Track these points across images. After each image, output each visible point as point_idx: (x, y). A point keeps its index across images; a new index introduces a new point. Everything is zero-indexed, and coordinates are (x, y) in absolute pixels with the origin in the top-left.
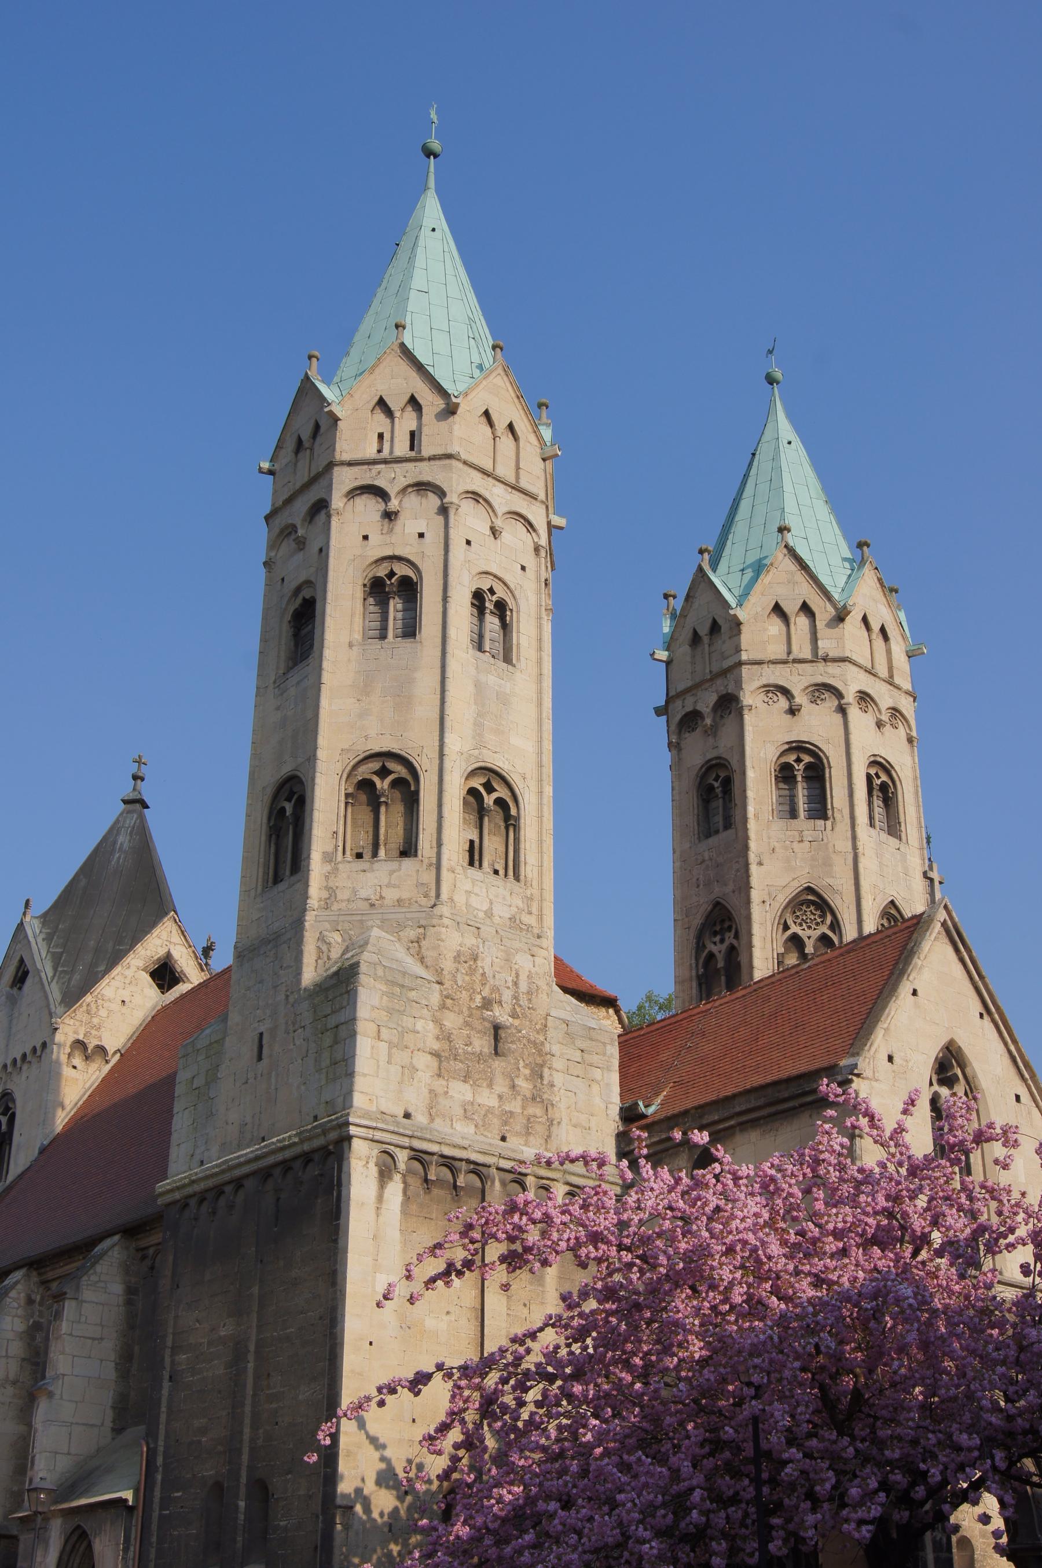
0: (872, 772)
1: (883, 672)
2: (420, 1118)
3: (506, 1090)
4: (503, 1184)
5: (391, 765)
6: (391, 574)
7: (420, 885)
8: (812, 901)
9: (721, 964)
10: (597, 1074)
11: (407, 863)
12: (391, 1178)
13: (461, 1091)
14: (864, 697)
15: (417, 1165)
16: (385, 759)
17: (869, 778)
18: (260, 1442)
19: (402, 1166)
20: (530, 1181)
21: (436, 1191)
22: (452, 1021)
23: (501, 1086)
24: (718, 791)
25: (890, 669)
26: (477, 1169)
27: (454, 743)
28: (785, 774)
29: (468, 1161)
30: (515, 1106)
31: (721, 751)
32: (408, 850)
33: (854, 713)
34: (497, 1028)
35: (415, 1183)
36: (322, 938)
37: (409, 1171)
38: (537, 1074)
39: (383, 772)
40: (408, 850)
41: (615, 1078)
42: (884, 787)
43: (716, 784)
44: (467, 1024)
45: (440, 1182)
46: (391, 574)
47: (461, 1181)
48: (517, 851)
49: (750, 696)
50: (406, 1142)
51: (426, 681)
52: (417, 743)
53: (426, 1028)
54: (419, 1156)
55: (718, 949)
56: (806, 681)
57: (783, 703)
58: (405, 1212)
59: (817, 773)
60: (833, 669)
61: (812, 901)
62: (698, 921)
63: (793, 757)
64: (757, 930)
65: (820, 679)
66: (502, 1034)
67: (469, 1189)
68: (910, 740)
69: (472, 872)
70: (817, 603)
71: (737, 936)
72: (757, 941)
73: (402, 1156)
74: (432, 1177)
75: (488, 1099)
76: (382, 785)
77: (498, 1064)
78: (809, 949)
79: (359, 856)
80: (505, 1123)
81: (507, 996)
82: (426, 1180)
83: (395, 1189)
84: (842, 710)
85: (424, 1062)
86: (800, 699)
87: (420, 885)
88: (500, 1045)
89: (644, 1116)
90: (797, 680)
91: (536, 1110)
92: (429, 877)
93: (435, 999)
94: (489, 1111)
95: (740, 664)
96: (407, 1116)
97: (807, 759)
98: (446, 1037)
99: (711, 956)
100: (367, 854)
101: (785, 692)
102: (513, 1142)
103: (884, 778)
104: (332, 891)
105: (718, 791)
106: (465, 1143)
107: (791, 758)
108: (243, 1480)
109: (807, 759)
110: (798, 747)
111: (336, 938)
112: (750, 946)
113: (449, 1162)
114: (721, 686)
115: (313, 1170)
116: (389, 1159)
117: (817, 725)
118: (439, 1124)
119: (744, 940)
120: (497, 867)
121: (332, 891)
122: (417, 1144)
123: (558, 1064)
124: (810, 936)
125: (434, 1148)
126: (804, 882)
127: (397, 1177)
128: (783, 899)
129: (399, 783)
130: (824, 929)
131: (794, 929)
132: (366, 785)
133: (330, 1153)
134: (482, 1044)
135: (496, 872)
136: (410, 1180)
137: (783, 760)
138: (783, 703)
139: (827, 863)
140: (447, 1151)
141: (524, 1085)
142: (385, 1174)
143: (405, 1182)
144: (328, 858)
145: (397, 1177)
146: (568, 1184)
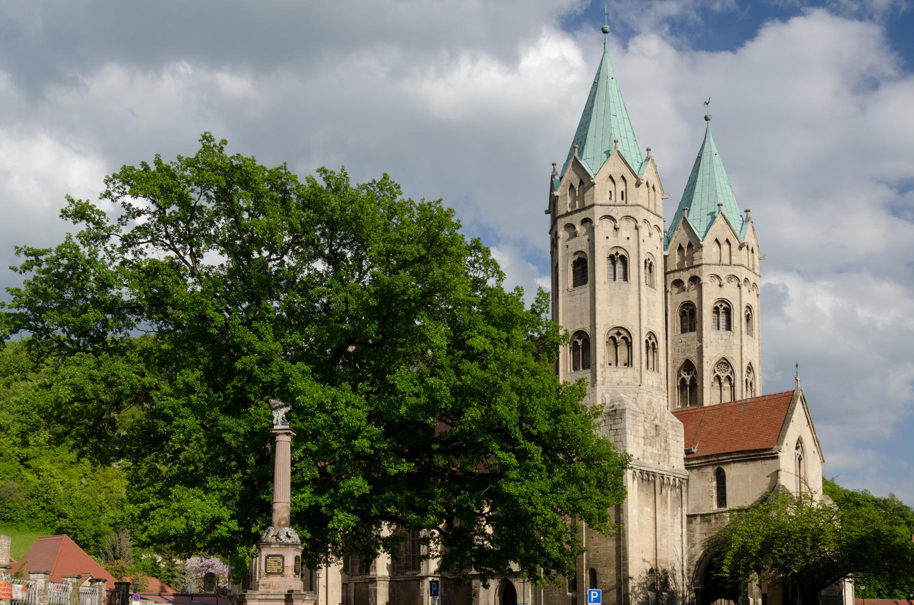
1: (751, 268)
2: (641, 459)
5: (621, 331)
6: (617, 254)
7: (634, 378)
8: (725, 363)
9: (688, 383)
11: (630, 370)
14: (746, 280)
16: (619, 329)
22: (647, 425)
23: (658, 447)
25: (753, 265)
26: (654, 474)
27: (644, 324)
28: (716, 310)
30: (661, 453)
32: (629, 363)
33: (743, 287)
36: (603, 396)
38: (666, 441)
39: (619, 334)
40: (629, 363)
46: (617, 254)
48: (658, 361)
49: (705, 279)
51: (633, 300)
52: (631, 325)
53: (641, 429)
54: (641, 472)
55: (688, 378)
56: (726, 274)
57: (717, 282)
59: (728, 311)
60: (737, 269)
61: (725, 363)
62: (679, 365)
64: (705, 373)
65: (732, 273)
68: (758, 295)
70: (732, 240)
71: (695, 373)
72: (705, 377)
73: (638, 472)
76: (618, 339)
77: (657, 439)
78: (722, 381)
79: (610, 364)
81: (658, 415)
83: (636, 481)
84: (739, 286)
85: (641, 441)
86: (724, 281)
87: (634, 378)
90: (724, 273)
91: (666, 453)
92: (637, 375)
93: (643, 419)
95: (702, 264)
97: (725, 305)
98: (645, 431)
99: (683, 379)
100: (614, 363)
101: (718, 277)
104: (604, 378)
107: (718, 305)
109: (725, 305)
110: (722, 301)
111: (607, 396)
112: (702, 379)
113: (648, 473)
114: (693, 272)
117: (730, 292)
118: (645, 461)
119: (699, 376)
121: (604, 378)
123: (670, 437)
124: (723, 375)
126: (722, 355)
128: (714, 361)
129: (624, 338)
130: (728, 373)
131: (718, 373)
132: (613, 338)
134: (653, 433)
138: (717, 282)
139: (731, 348)
141: (663, 445)
142: (634, 479)
144: (602, 366)
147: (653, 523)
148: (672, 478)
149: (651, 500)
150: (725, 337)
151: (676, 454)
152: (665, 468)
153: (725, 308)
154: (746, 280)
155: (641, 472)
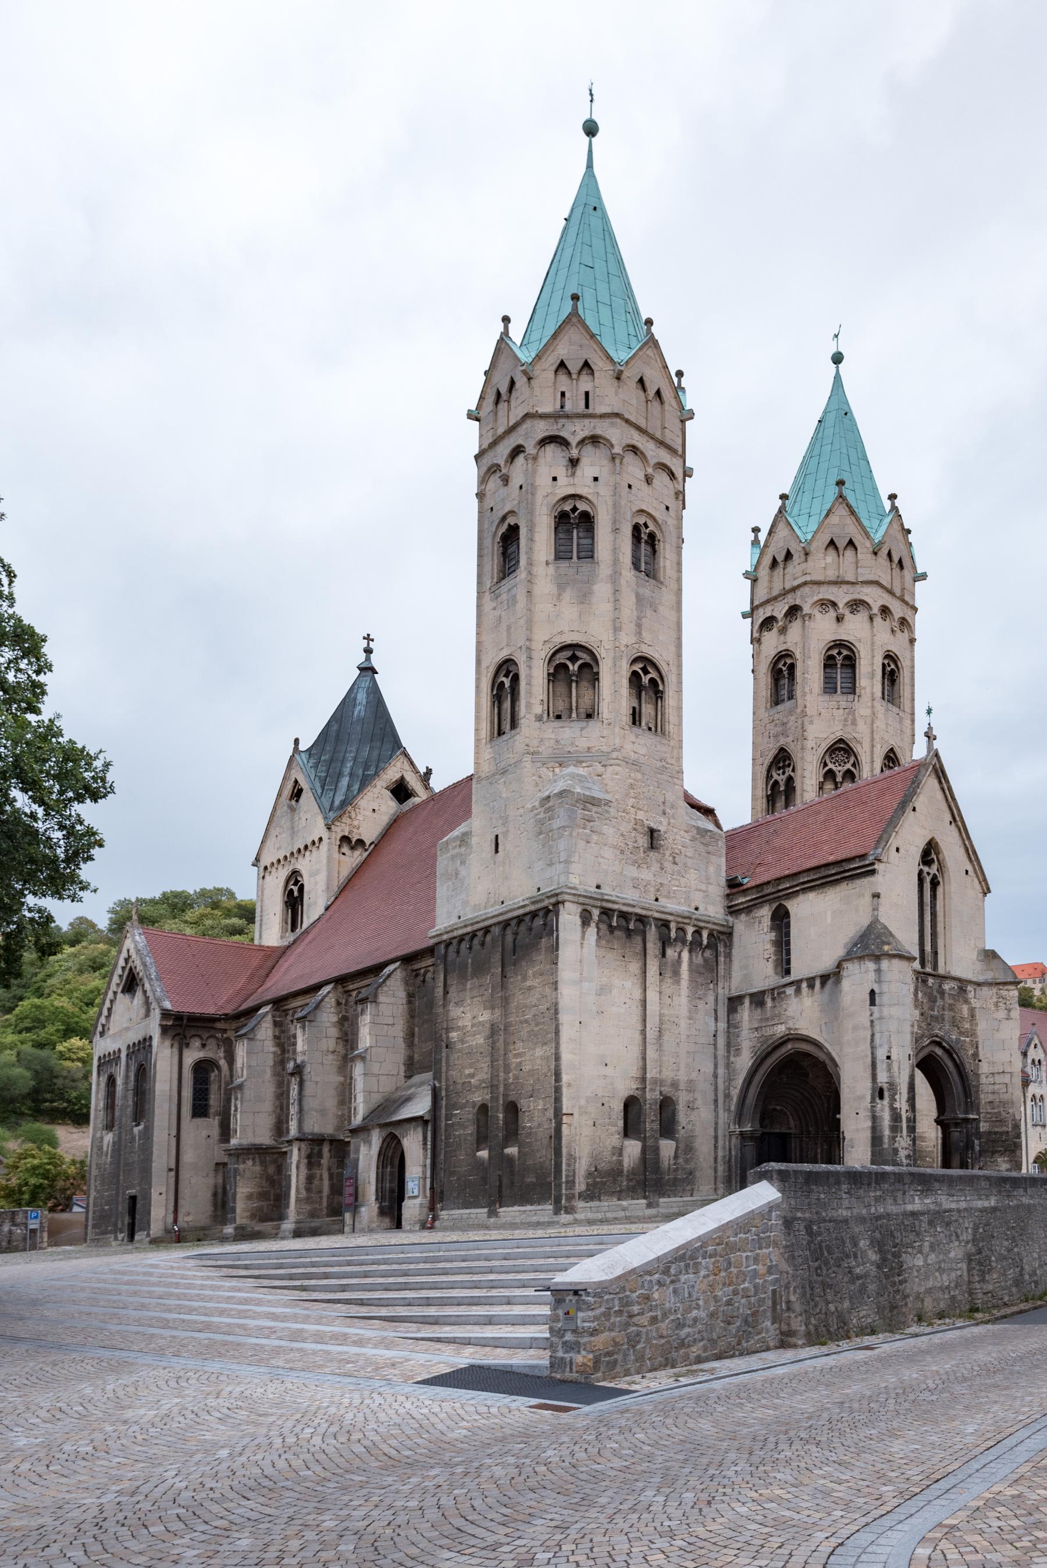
0: (886, 662)
3: (658, 869)
4: (656, 926)
10: (713, 858)
12: (589, 925)
13: (632, 871)
15: (604, 917)
17: (883, 664)
18: (511, 1081)
19: (596, 918)
20: (673, 925)
21: (617, 933)
23: (655, 867)
24: (786, 673)
26: (642, 919)
28: (829, 663)
29: (636, 914)
31: (789, 646)
34: (652, 832)
35: (604, 927)
37: (600, 921)
41: (723, 861)
42: (892, 672)
43: (784, 669)
44: (635, 829)
45: (618, 927)
47: (631, 926)
50: (599, 904)
54: (606, 912)
58: (597, 946)
59: (851, 663)
63: (836, 651)
66: (655, 835)
67: (635, 931)
69: (635, 729)
74: (614, 924)
75: (646, 875)
80: (658, 890)
82: (610, 926)
88: (655, 842)
89: (741, 885)
94: (648, 883)
96: (598, 887)
97: (845, 652)
102: (663, 901)
103: (893, 666)
105: (786, 673)
106: (635, 903)
108: (501, 1102)
109: (845, 652)
113: (624, 916)
115: (539, 922)
116: (587, 914)
120: (651, 725)
122: (605, 904)
125: (616, 907)
127: (593, 925)
133: (549, 911)
135: (650, 729)
136: (601, 926)
137: (830, 653)
140: (625, 909)
143: (598, 928)
145: (593, 925)
146: (694, 926)
147: (637, 1011)
148: (690, 930)
149: (635, 967)
150: (843, 704)
151: (703, 887)
152: (673, 906)
153: (847, 658)
154: (885, 610)
155: (606, 912)
